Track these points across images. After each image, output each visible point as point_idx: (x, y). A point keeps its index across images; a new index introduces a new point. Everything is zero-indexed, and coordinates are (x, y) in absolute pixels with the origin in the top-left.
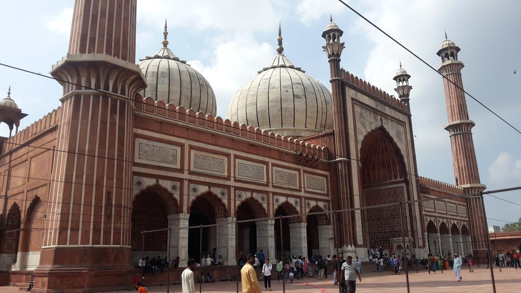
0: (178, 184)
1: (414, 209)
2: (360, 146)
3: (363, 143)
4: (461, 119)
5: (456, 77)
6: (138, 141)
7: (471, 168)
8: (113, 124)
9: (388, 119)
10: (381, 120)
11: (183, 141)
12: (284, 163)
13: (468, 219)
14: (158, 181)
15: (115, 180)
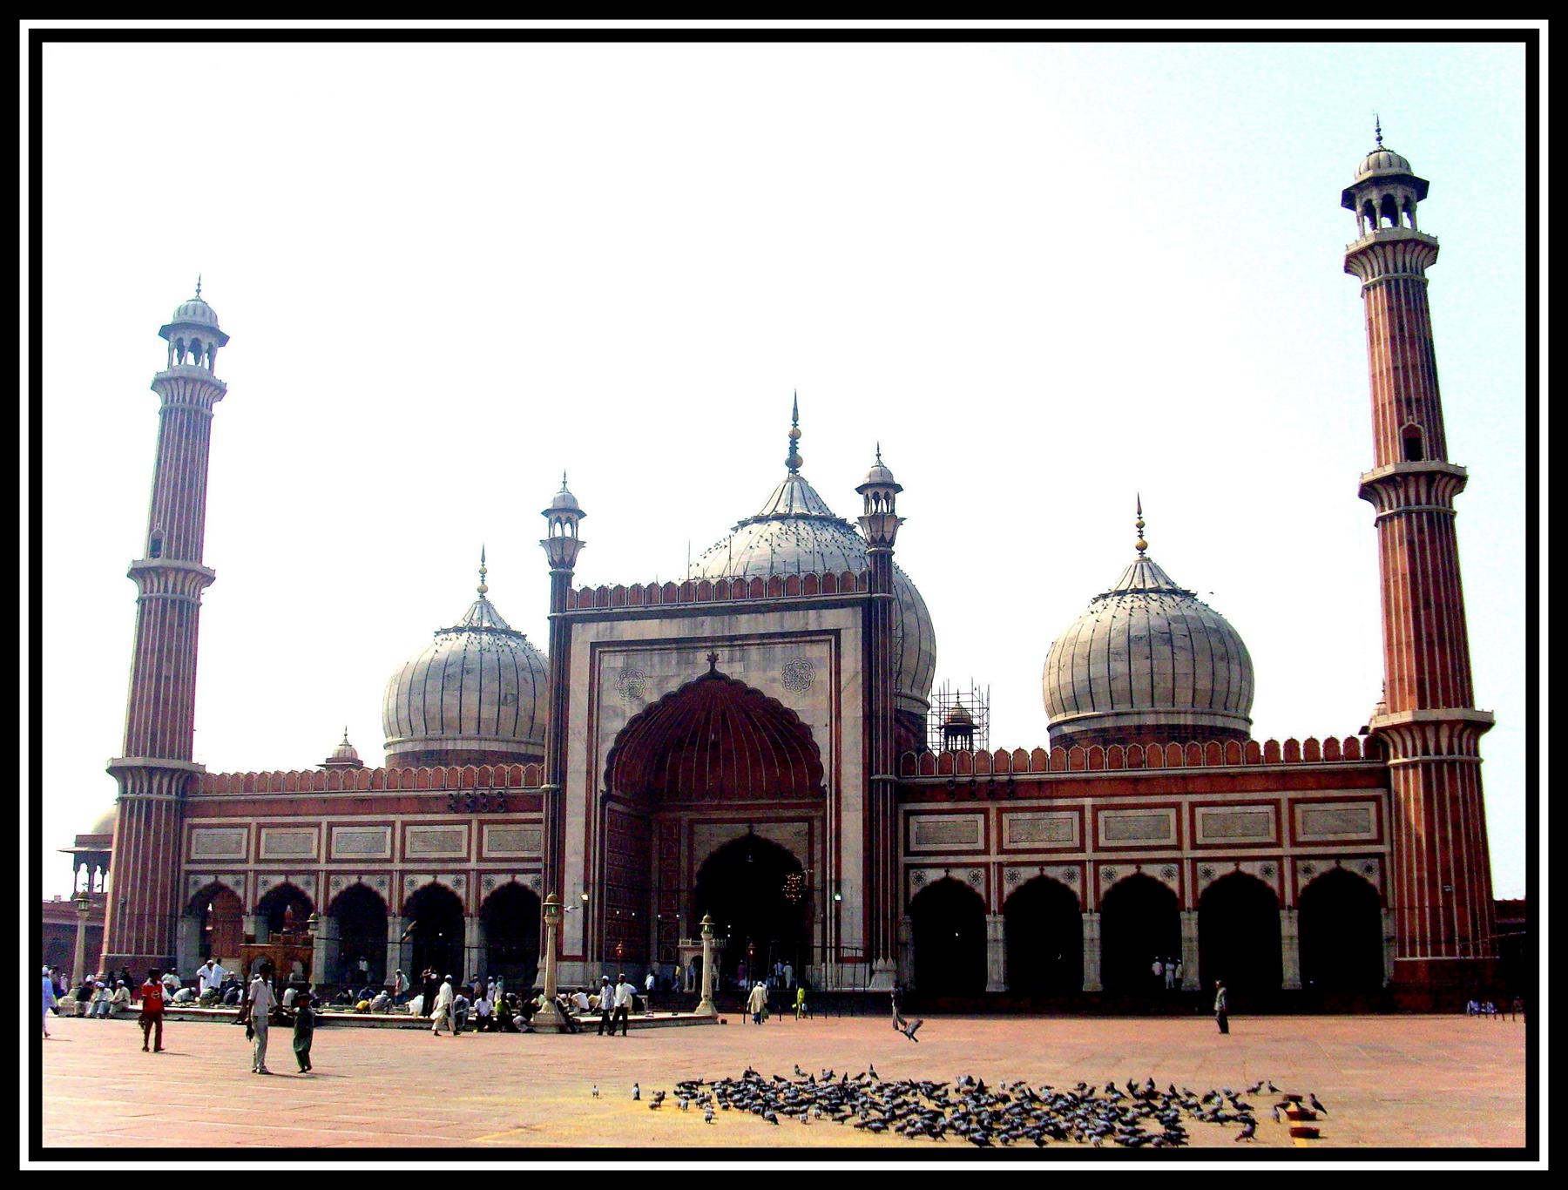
0: (242, 877)
1: (833, 862)
2: (607, 746)
3: (622, 736)
4: (1379, 465)
5: (1375, 298)
6: (196, 832)
7: (1400, 651)
8: (130, 828)
9: (745, 647)
10: (713, 659)
11: (248, 820)
12: (429, 817)
13: (1384, 848)
14: (216, 877)
15: (129, 889)
